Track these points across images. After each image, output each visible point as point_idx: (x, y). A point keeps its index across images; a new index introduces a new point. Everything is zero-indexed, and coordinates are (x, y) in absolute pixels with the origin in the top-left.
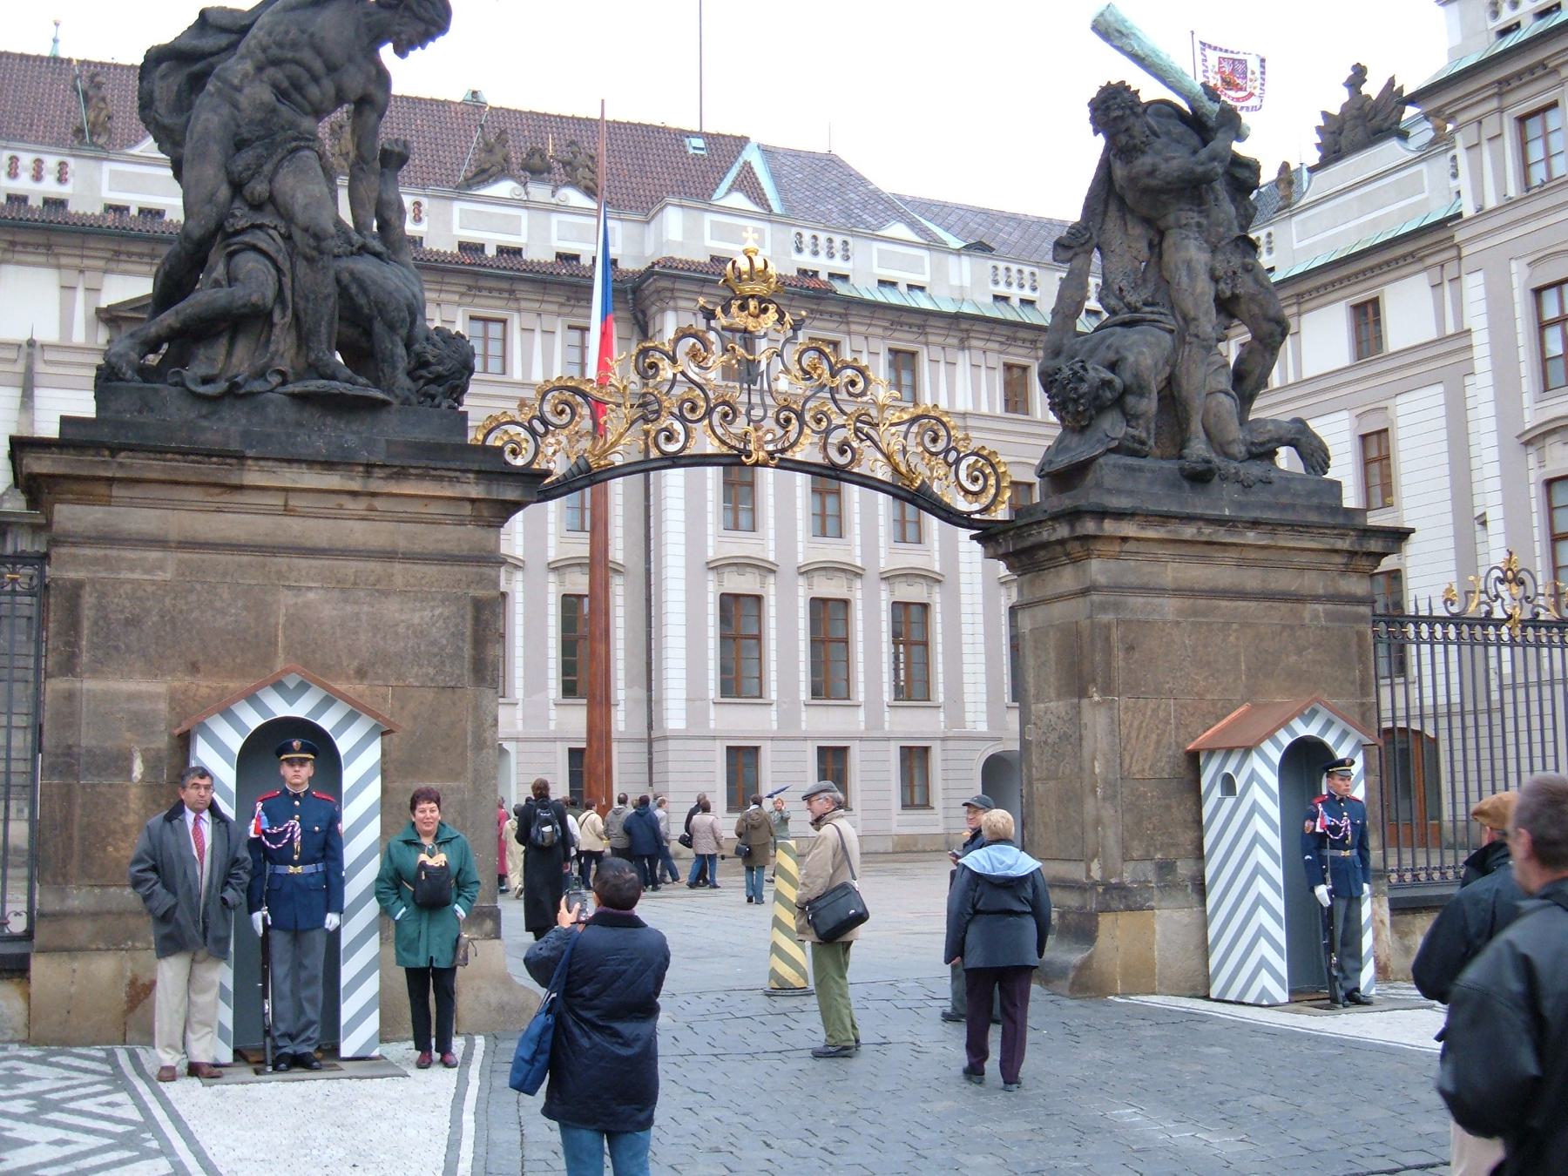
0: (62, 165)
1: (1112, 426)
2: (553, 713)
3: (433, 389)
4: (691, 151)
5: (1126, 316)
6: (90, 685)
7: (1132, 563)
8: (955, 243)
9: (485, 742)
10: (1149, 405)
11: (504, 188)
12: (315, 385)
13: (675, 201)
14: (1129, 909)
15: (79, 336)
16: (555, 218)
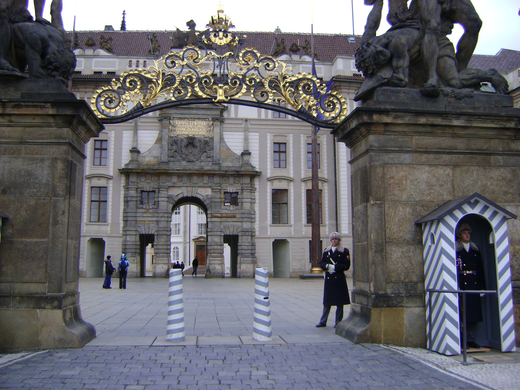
0: (145, 62)
1: (386, 74)
2: (304, 229)
3: (55, 73)
4: (350, 42)
5: (398, 24)
7: (393, 136)
9: (58, 221)
10: (405, 63)
11: (284, 57)
13: (340, 56)
14: (388, 306)
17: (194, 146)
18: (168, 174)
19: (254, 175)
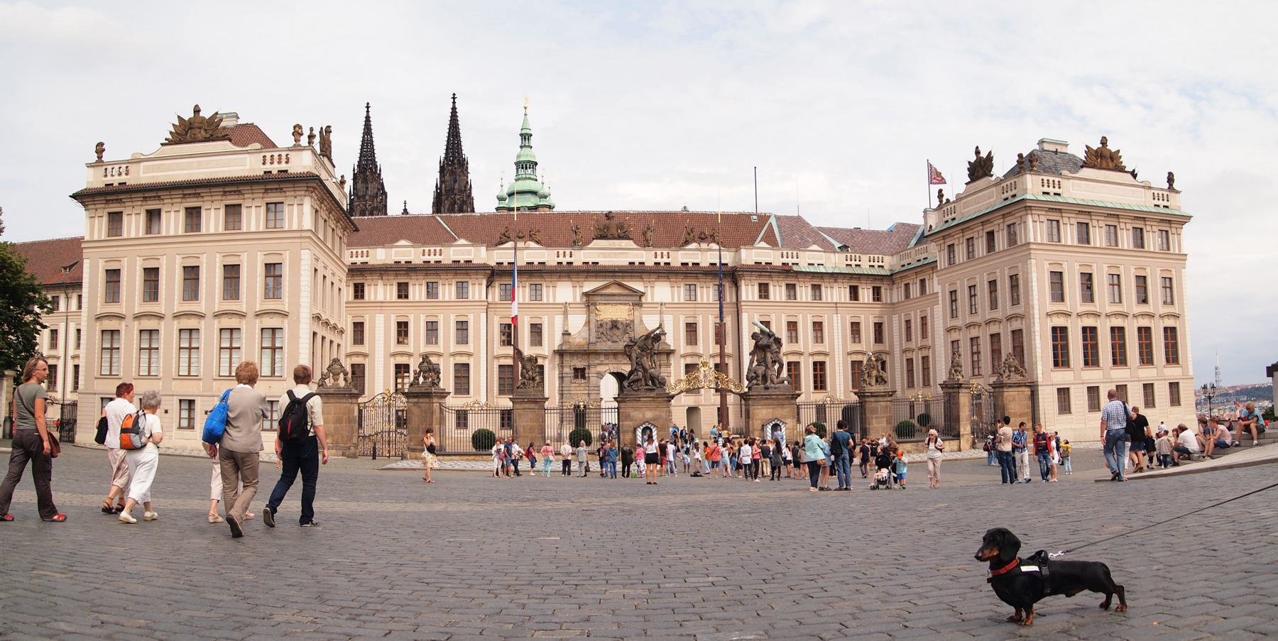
0: (571, 252)
1: (755, 382)
6: (625, 423)
8: (837, 245)
10: (760, 378)
11: (694, 245)
12: (647, 387)
15: (578, 300)
16: (709, 252)
17: (618, 329)
18: (597, 353)
19: (669, 353)
